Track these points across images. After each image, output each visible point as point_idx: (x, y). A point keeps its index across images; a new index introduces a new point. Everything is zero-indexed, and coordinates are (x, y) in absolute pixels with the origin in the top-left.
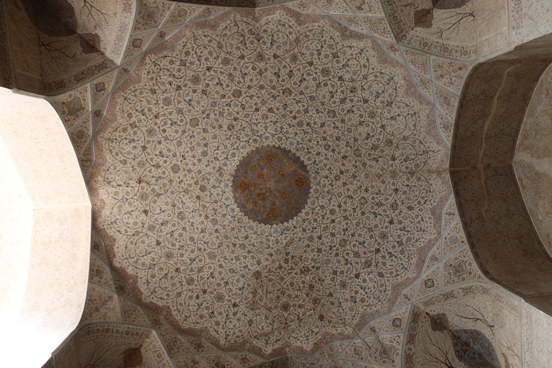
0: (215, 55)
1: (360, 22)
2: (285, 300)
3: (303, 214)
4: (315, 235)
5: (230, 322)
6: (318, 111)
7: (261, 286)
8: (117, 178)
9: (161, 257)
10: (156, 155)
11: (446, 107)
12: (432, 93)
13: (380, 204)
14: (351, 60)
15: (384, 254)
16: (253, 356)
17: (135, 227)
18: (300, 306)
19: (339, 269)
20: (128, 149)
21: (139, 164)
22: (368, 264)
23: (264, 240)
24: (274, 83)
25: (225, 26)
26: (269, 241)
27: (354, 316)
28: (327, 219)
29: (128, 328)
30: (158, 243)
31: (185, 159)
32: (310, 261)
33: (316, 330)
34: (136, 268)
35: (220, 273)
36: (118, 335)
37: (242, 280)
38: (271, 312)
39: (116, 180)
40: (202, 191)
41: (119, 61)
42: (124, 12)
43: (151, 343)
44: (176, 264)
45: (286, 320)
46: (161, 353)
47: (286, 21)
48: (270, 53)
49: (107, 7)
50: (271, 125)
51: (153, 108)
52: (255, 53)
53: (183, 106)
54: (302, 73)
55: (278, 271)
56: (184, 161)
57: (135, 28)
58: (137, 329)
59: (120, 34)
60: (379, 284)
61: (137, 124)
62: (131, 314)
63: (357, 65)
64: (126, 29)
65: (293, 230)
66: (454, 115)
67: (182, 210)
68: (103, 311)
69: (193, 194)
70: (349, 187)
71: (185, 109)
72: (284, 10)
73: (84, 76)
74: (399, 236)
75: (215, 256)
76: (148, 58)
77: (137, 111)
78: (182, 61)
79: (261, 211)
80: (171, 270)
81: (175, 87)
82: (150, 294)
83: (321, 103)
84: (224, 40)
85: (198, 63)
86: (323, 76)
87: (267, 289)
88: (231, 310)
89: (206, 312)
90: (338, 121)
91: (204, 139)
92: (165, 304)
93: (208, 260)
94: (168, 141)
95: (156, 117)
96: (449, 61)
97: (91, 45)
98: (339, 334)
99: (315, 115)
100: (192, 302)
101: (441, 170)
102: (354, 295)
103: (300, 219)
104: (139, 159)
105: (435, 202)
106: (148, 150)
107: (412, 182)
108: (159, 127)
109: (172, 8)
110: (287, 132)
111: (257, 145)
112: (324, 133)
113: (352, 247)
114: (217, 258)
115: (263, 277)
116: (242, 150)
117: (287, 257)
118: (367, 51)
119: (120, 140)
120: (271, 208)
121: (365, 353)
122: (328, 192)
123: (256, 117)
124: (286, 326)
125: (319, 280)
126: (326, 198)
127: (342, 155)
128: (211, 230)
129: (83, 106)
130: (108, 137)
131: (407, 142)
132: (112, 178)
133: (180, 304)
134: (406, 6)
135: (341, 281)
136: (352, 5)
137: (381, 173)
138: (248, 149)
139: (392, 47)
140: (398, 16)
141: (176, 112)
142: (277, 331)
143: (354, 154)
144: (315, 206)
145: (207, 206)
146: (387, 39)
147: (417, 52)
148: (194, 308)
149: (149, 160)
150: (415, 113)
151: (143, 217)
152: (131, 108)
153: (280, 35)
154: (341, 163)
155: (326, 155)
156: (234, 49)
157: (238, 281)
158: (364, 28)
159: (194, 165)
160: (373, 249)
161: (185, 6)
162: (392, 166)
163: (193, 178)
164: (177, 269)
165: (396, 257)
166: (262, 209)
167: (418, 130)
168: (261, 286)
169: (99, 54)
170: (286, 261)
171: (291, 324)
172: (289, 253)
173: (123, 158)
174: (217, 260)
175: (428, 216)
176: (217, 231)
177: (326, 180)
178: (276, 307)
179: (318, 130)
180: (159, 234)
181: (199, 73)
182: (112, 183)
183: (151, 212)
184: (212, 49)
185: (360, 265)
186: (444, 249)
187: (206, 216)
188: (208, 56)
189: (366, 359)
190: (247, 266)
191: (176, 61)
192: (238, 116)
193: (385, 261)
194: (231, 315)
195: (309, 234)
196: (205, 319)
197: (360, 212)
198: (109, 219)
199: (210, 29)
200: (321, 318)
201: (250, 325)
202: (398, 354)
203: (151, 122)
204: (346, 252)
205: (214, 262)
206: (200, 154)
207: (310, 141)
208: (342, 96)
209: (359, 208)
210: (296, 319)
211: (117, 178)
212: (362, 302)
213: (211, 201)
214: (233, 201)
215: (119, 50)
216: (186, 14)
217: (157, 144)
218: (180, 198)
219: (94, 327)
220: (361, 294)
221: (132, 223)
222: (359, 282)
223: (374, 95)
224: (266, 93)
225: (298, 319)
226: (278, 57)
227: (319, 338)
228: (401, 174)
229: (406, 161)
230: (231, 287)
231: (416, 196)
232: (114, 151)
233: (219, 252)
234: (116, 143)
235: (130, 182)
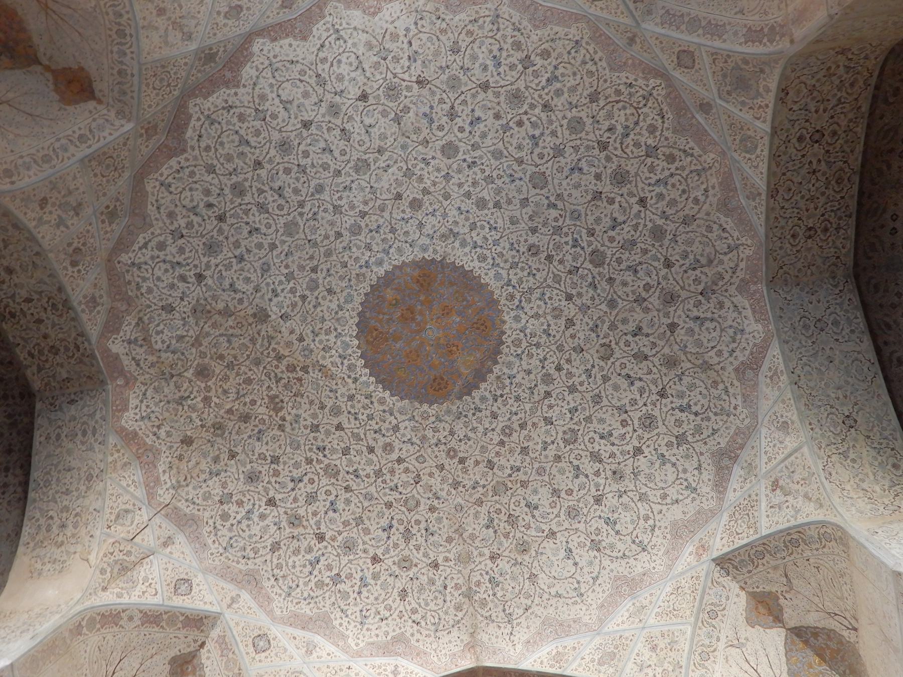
0: (669, 212)
1: (748, 485)
2: (217, 371)
4: (343, 419)
5: (166, 271)
8: (424, 37)
9: (280, 131)
10: (473, 111)
13: (407, 535)
15: (315, 549)
16: (101, 319)
18: (207, 400)
19: (282, 466)
20: (481, 56)
21: (455, 78)
22: (295, 520)
23: (327, 325)
24: (621, 327)
25: (728, 227)
26: (326, 334)
27: (194, 503)
29: (133, 75)
30: (306, 125)
31: (469, 167)
32: (294, 411)
33: (162, 433)
34: (255, 84)
36: (116, 56)
37: (250, 288)
38: (193, 345)
40: (411, 203)
42: (745, 30)
43: (107, 120)
45: (179, 375)
46: (90, 142)
47: (744, 345)
48: (680, 317)
50: (542, 324)
52: (678, 287)
53: (570, 157)
54: (644, 377)
55: (273, 354)
56: (465, 165)
57: (715, 55)
59: (703, 23)
60: (258, 545)
61: (531, 69)
62: (162, 80)
63: (666, 482)
64: (712, 35)
65: (349, 377)
67: (373, 168)
68: (161, 22)
69: (404, 187)
72: (764, 340)
74: (350, 576)
75: (290, 235)
76: (658, 82)
77: (556, 68)
78: (656, 148)
80: (258, 151)
81: (604, 139)
84: (699, 226)
85: (653, 181)
86: (640, 419)
87: (236, 336)
89: (183, 223)
90: (558, 449)
91: (509, 202)
93: (282, 221)
95: (546, 107)
96: (683, 664)
98: (158, 479)
100: (198, 195)
101: (478, 649)
102: (234, 498)
103: (372, 388)
104: (464, 79)
106: (482, 96)
108: (526, 113)
109: (758, 123)
110: (531, 356)
111: (503, 302)
112: (534, 424)
116: (492, 273)
118: (694, 499)
120: (388, 333)
121: (121, 531)
122: (424, 438)
123: (555, 297)
124: (167, 376)
125: (259, 432)
126: (413, 434)
127: (495, 460)
128: (339, 224)
130: (500, 12)
133: (192, 174)
134: (786, 576)
135: (260, 472)
136: (781, 471)
137: (465, 535)
138: (494, 285)
139: (703, 547)
140: (764, 561)
142: (155, 359)
144: (398, 415)
146: (718, 539)
147: (698, 598)
148: (188, 200)
150: (582, 595)
152: (560, 55)
153: (714, 334)
154: (479, 458)
155: (493, 430)
156: (683, 247)
157: (247, 280)
158: (738, 494)
159: (460, 185)
160: (323, 529)
161: (764, 150)
166: (387, 317)
167: (550, 602)
168: (239, 325)
170: (291, 368)
171: (172, 384)
174: (283, 238)
175: (390, 631)
176: (339, 235)
177: (446, 433)
178: (203, 355)
179: (539, 413)
182: (413, 27)
183: (365, 107)
184: (680, 206)
187: (366, 213)
188: (668, 198)
189: (109, 535)
190: (276, 296)
192: (556, 263)
193: (303, 553)
194: (179, 271)
196: (168, 222)
197: (391, 499)
198: (344, 25)
200: (187, 441)
201: (163, 308)
202: (119, 596)
203: (536, 96)
204: (316, 478)
206: (480, 195)
207: (518, 399)
208: (605, 455)
209: (398, 496)
210: (182, 393)
211: (424, 37)
212: (222, 516)
214: (396, 263)
215: (671, 24)
216: (747, 152)
217: (492, 112)
218: (396, 162)
219: (125, 7)
220: (237, 513)
221: (340, 71)
223: (610, 515)
224: (602, 313)
225: (182, 398)
226: (672, 332)
227: (147, 440)
228: (466, 572)
230: (235, 268)
231: (427, 604)
232: (476, 28)
233: (299, 242)
234: (491, 30)
235: (419, 62)
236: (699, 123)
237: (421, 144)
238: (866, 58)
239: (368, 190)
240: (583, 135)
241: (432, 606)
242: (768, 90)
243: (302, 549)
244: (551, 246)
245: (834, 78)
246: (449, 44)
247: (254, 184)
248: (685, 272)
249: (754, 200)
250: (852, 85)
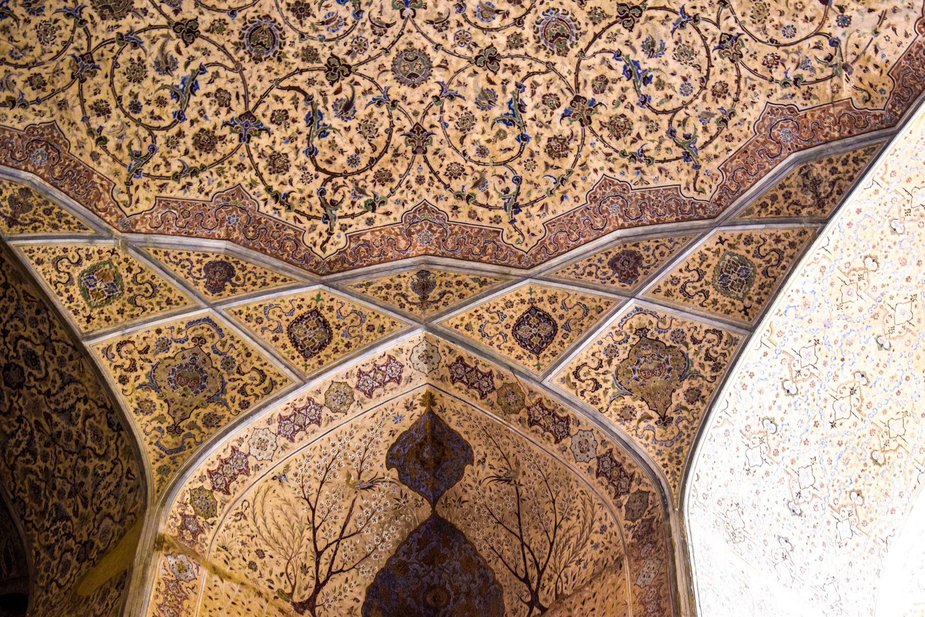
0: (128, 54)
8: (804, 29)
20: (674, 65)
39: (812, 28)
41: (410, 341)
42: (252, 462)
49: (281, 521)
51: (471, 93)
57: (270, 386)
59: (326, 411)
61: (565, 104)
64: (297, 412)
73: (537, 413)
76: (331, 250)
77: (523, 138)
78: (245, 138)
81: (345, 83)
84: (57, 72)
85: (202, 80)
95: (491, 59)
97: (430, 454)
108: (519, 22)
109: (114, 337)
119: (665, 118)
132: (818, 47)
141: (421, 12)
152: (531, 165)
161: (71, 305)
169: (443, 410)
173: (719, 62)
181: (230, 49)
182: (838, 33)
184: (119, 78)
188: (152, 73)
191: (261, 155)
199: (67, 144)
203: (523, 64)
215: (377, 369)
216: (93, 269)
234: (683, 123)
236: (211, 237)
238: (49, 548)
242: (143, 407)
245: (67, 488)
249: (12, 200)
250: (35, 488)
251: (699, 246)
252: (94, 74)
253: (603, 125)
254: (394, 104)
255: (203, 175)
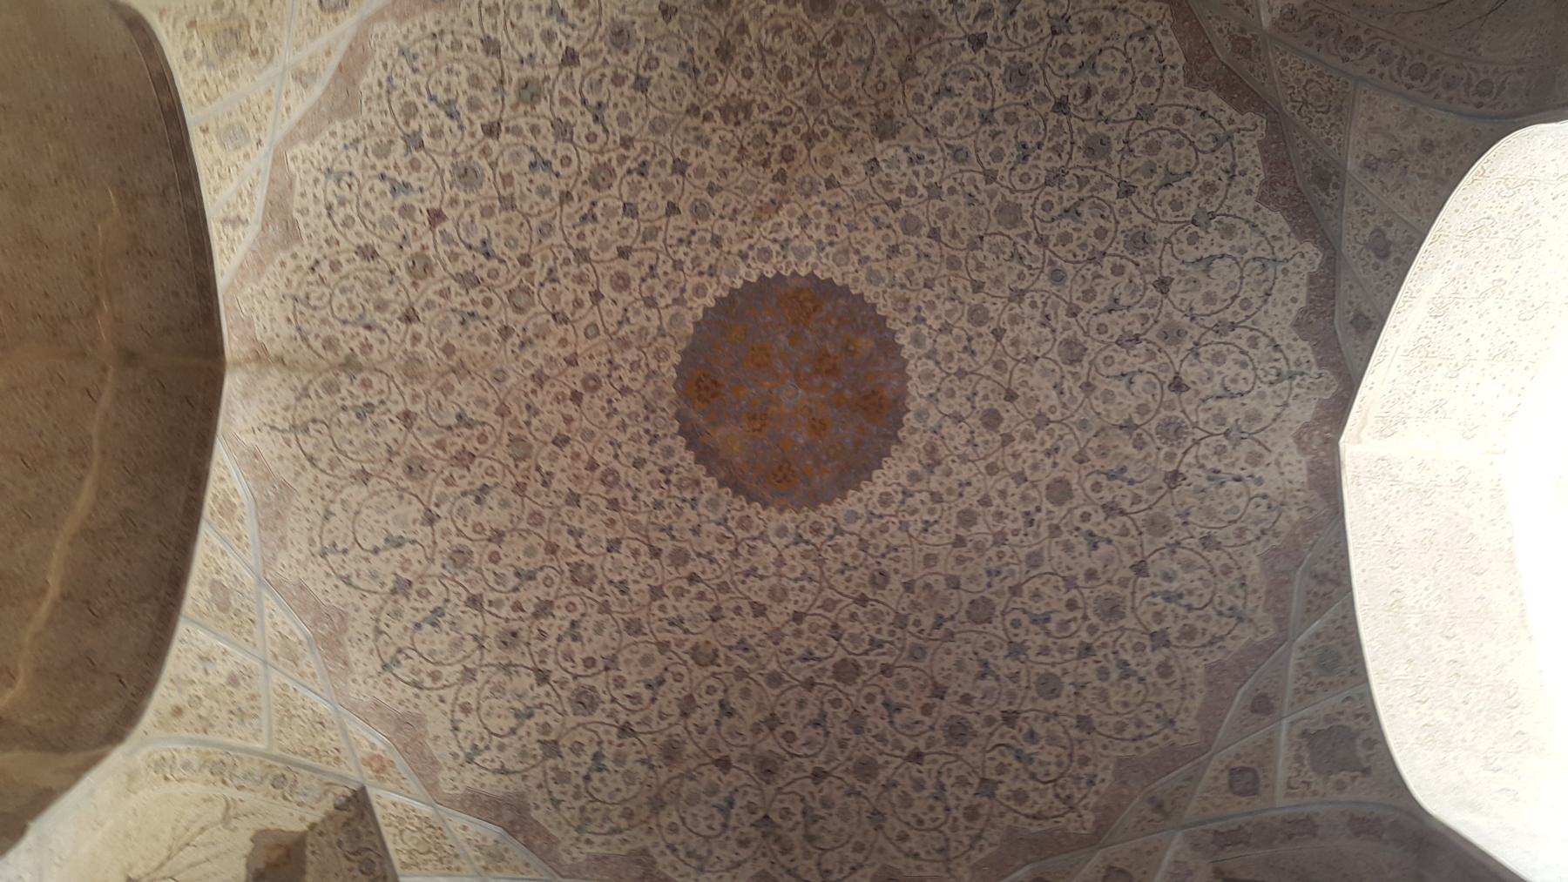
0: (895, 794)
2: (816, 27)
3: (714, 292)
4: (685, 219)
6: (623, 587)
7: (882, 86)
9: (1167, 241)
10: (1109, 541)
11: (224, 578)
12: (267, 622)
13: (468, 280)
14: (506, 730)
15: (473, 117)
17: (1224, 348)
20: (1188, 577)
21: (1165, 528)
22: (530, 92)
24: (738, 686)
26: (828, 227)
28: (640, 264)
29: (1345, 60)
30: (1163, 285)
31: (1027, 514)
32: (716, 139)
35: (997, 156)
37: (935, 120)
39: (1245, 498)
40: (996, 412)
44: (1125, 211)
50: (766, 568)
51: (1092, 677)
52: (781, 783)
53: (1004, 665)
54: (655, 707)
55: (818, 129)
56: (1031, 508)
58: (1319, 48)
61: (1146, 640)
62: (1318, 97)
63: (488, 714)
65: (751, 247)
66: (201, 551)
67: (1066, 368)
69: (1023, 409)
70: (560, 350)
71: (1001, 653)
74: (415, 165)
75: (1000, 210)
76: (1089, 825)
77: (1141, 680)
78: (991, 795)
79: (834, 322)
80: (1148, 196)
81: (1020, 722)
82: (1236, 136)
83: (609, 612)
84: (866, 833)
85: (944, 779)
87: (865, 76)
88: (995, 28)
89: (1076, 40)
90: (568, 553)
92: (1199, 95)
93: (1026, 203)
94: (1067, 573)
95: (1087, 650)
99: (631, 577)
100: (1110, 79)
101: (253, 367)
103: (725, 280)
105: (283, 264)
106: (1128, 560)
107: (353, 337)
108: (1085, 618)
110: (721, 539)
111: (813, 516)
112: (613, 522)
113: (574, 158)
114: (995, 205)
115: (868, 118)
116: (859, 508)
117: (784, 166)
118: (455, 756)
122: (625, 344)
123: (803, 595)
125: (696, 70)
126: (636, 328)
127: (568, 450)
128: (994, 291)
129: (1304, 742)
130: (1245, 625)
131: (357, 466)
133: (1148, 81)
135: (626, 52)
138: (840, 508)
139: (380, 767)
143: (531, 447)
144: (672, 311)
145: (990, 367)
146: (396, 797)
147: (307, 761)
148: (1110, 61)
149: (1134, 532)
150: (323, 555)
151: (1190, 373)
152: (1158, 692)
153: (702, 828)
154: (575, 425)
155: (616, 456)
157: (949, 120)
159: (1003, 493)
160: (506, 138)
162: (415, 397)
163: (1015, 456)
164: (1127, 193)
165: (433, 98)
167: (318, 501)
168: (882, 86)
170: (788, 154)
172: (774, 180)
173: (1211, 555)
174: (999, 197)
177: (626, 381)
179: (629, 534)
180: (1155, 311)
182: (1261, 490)
185: (556, 94)
186: (268, 108)
187: (999, 338)
188: (915, 795)
192: (853, 608)
193: (471, 92)
195: (702, 225)
196: (1085, 17)
197: (536, 267)
198: (1296, 390)
203: (1106, 639)
205: (1007, 193)
206: (980, 520)
207: (658, 505)
208: (544, 623)
209: (537, 279)
213: (975, 378)
214: (911, 366)
218: (1064, 406)
221: (1229, 363)
222: (567, 37)
223: (448, 617)
226: (716, 762)
228: (389, 368)
229: (368, 405)
231: (343, 291)
233: (985, 221)
234: (1221, 603)
237: (1082, 450)
239: (1034, 352)
240: (1033, 693)
241: (340, 298)
243: (478, 93)
244: (880, 607)
246: (1219, 535)
247: (1098, 175)
248: (803, 800)
251: (1293, 662)
252: (885, 820)
253: (1178, 639)
254: (1056, 714)
255: (985, 835)
